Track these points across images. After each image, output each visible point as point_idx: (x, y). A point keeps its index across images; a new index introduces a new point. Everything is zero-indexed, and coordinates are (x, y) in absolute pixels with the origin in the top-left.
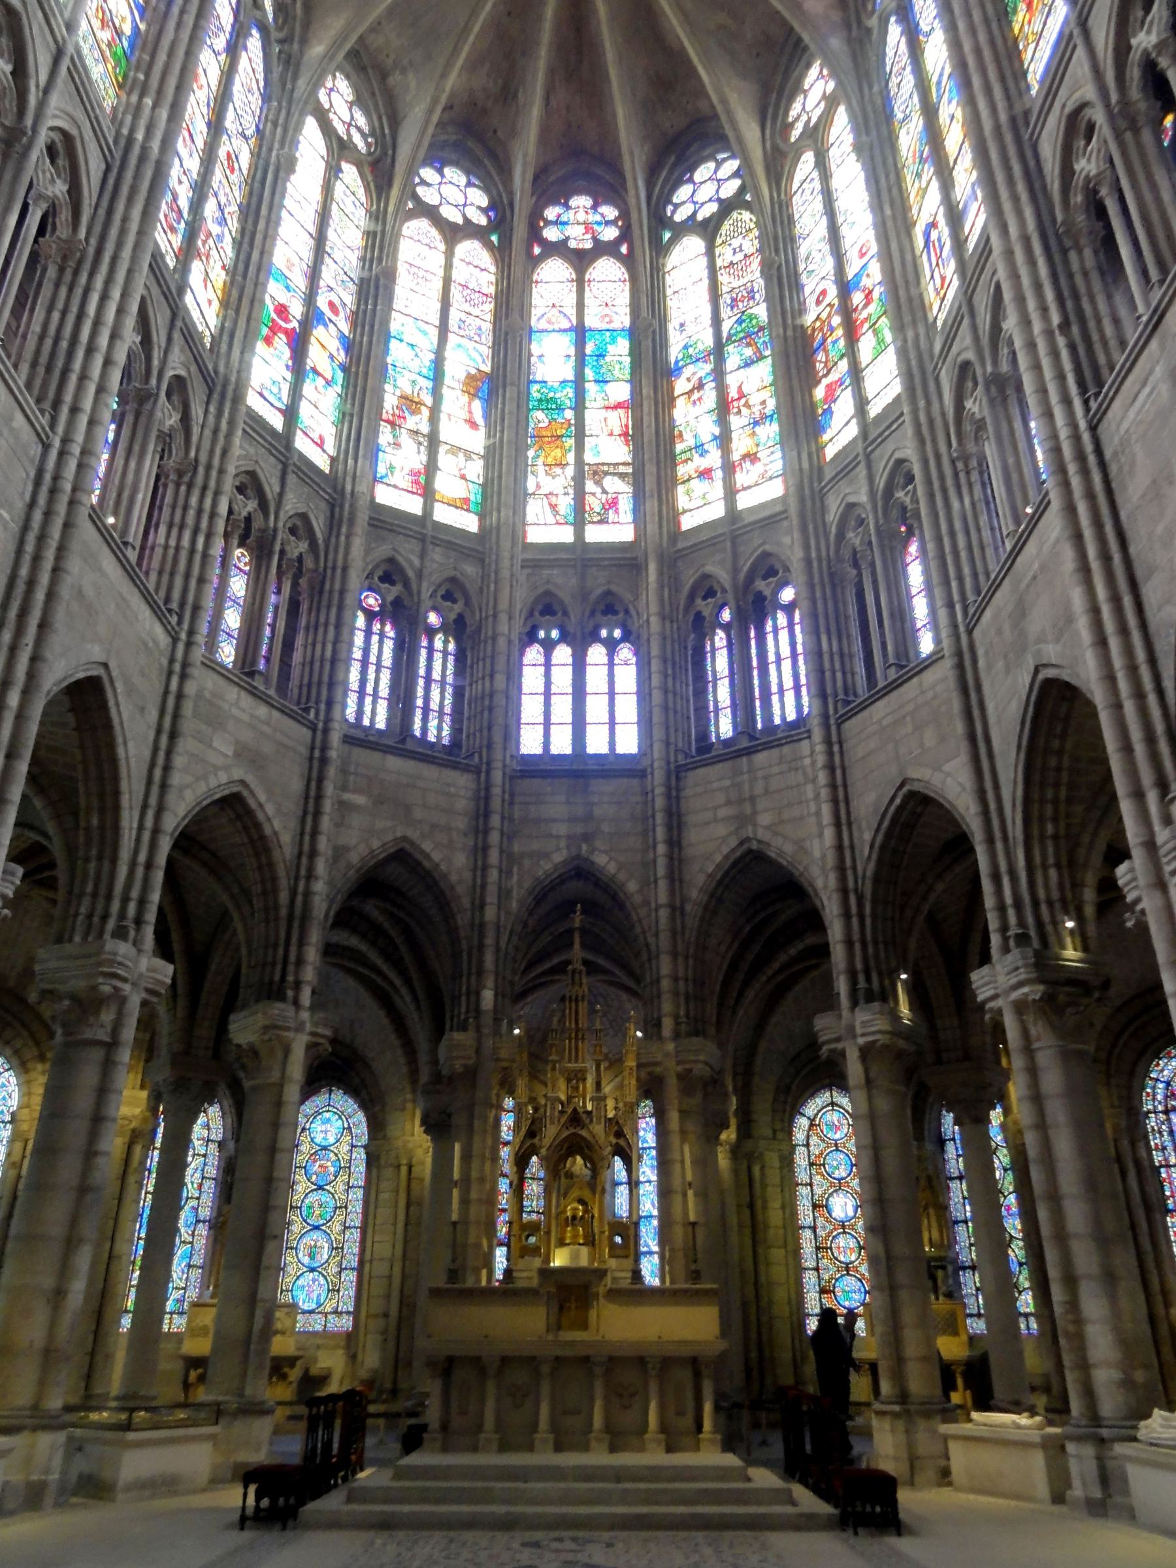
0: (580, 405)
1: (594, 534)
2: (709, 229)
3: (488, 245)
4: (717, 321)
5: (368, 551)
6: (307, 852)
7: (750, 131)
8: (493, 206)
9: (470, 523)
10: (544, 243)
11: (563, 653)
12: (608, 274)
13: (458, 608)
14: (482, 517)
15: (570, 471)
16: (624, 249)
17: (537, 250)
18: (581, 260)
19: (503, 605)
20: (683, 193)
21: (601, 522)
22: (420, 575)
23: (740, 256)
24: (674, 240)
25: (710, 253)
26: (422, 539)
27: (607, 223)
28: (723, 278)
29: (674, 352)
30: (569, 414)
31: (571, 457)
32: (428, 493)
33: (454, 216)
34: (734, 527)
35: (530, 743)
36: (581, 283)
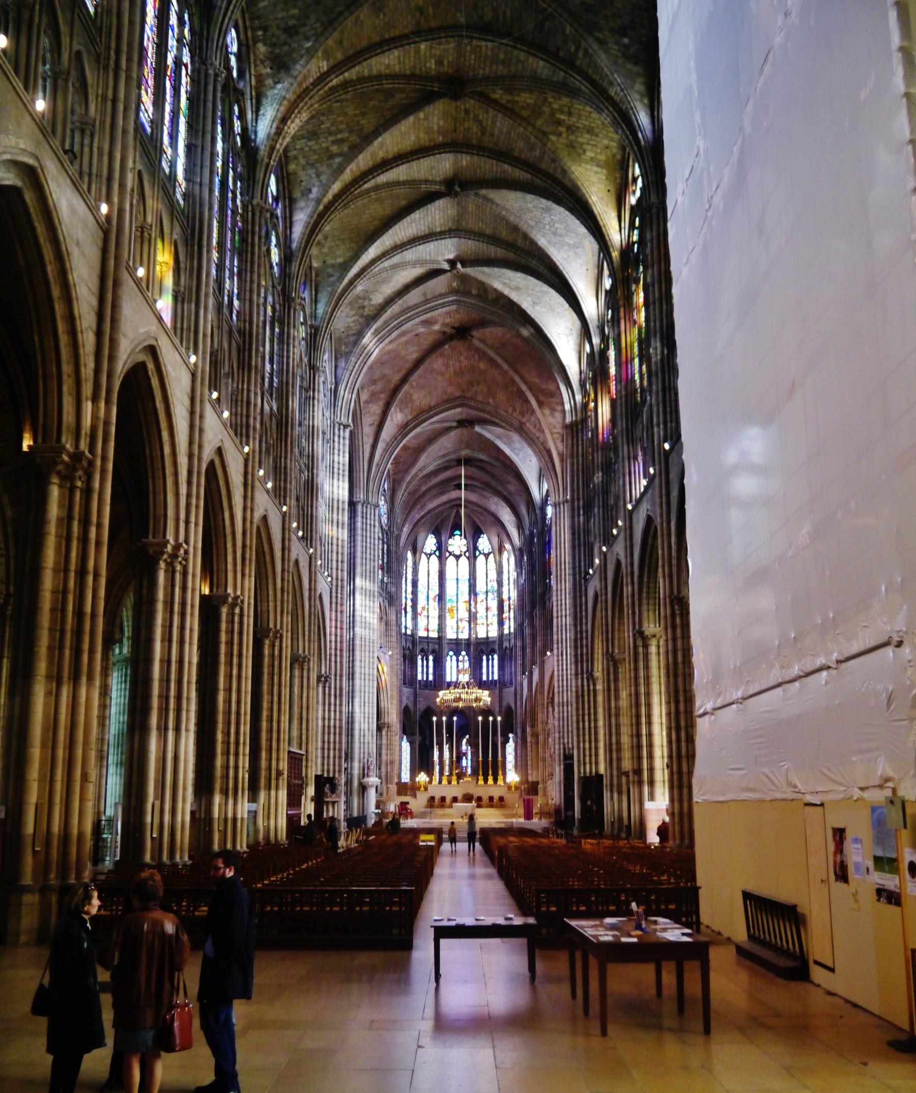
2: (487, 556)
6: (415, 712)
7: (495, 540)
8: (437, 542)
9: (434, 634)
11: (454, 658)
12: (464, 561)
16: (467, 554)
18: (457, 557)
20: (480, 540)
29: (478, 590)
30: (455, 604)
32: (428, 630)
33: (428, 552)
34: (487, 641)
35: (448, 679)
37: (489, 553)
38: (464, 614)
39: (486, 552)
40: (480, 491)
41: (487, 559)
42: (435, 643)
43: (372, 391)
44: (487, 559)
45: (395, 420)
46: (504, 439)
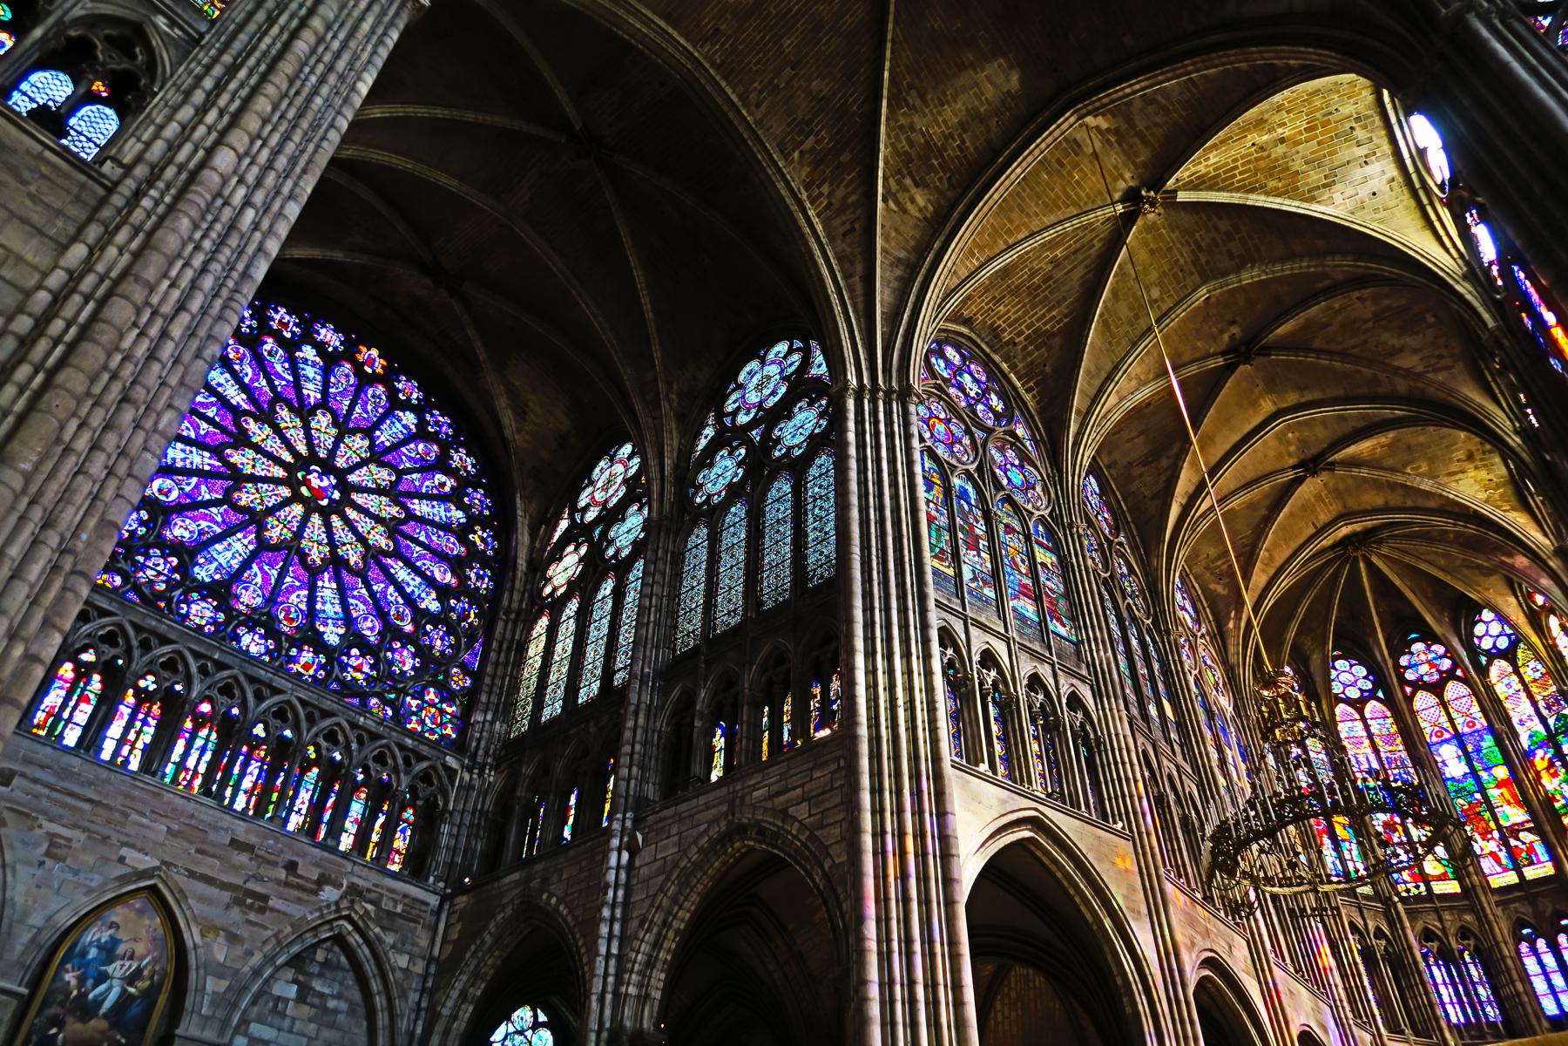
0: (1482, 789)
1: (1530, 873)
2: (1509, 655)
3: (1379, 700)
4: (1543, 721)
5: (1413, 929)
9: (1453, 887)
10: (1410, 683)
11: (1541, 944)
13: (1472, 942)
14: (1459, 878)
15: (1496, 834)
17: (1408, 690)
18: (1437, 689)
19: (1500, 938)
20: (1479, 629)
21: (1531, 863)
22: (1444, 930)
23: (1538, 675)
24: (1490, 663)
25: (1516, 671)
26: (1436, 910)
27: (1441, 657)
28: (1534, 690)
30: (1478, 796)
31: (1492, 824)
33: (1354, 693)
36: (1444, 705)
37: (1514, 645)
38: (1514, 815)
39: (1503, 643)
40: (1363, 447)
41: (1513, 661)
42: (1461, 910)
43: (813, 149)
44: (1513, 661)
45: (909, 206)
46: (1272, 184)
